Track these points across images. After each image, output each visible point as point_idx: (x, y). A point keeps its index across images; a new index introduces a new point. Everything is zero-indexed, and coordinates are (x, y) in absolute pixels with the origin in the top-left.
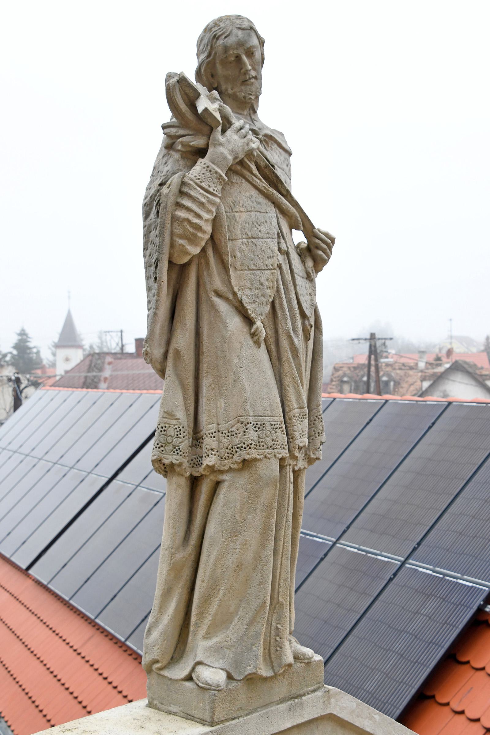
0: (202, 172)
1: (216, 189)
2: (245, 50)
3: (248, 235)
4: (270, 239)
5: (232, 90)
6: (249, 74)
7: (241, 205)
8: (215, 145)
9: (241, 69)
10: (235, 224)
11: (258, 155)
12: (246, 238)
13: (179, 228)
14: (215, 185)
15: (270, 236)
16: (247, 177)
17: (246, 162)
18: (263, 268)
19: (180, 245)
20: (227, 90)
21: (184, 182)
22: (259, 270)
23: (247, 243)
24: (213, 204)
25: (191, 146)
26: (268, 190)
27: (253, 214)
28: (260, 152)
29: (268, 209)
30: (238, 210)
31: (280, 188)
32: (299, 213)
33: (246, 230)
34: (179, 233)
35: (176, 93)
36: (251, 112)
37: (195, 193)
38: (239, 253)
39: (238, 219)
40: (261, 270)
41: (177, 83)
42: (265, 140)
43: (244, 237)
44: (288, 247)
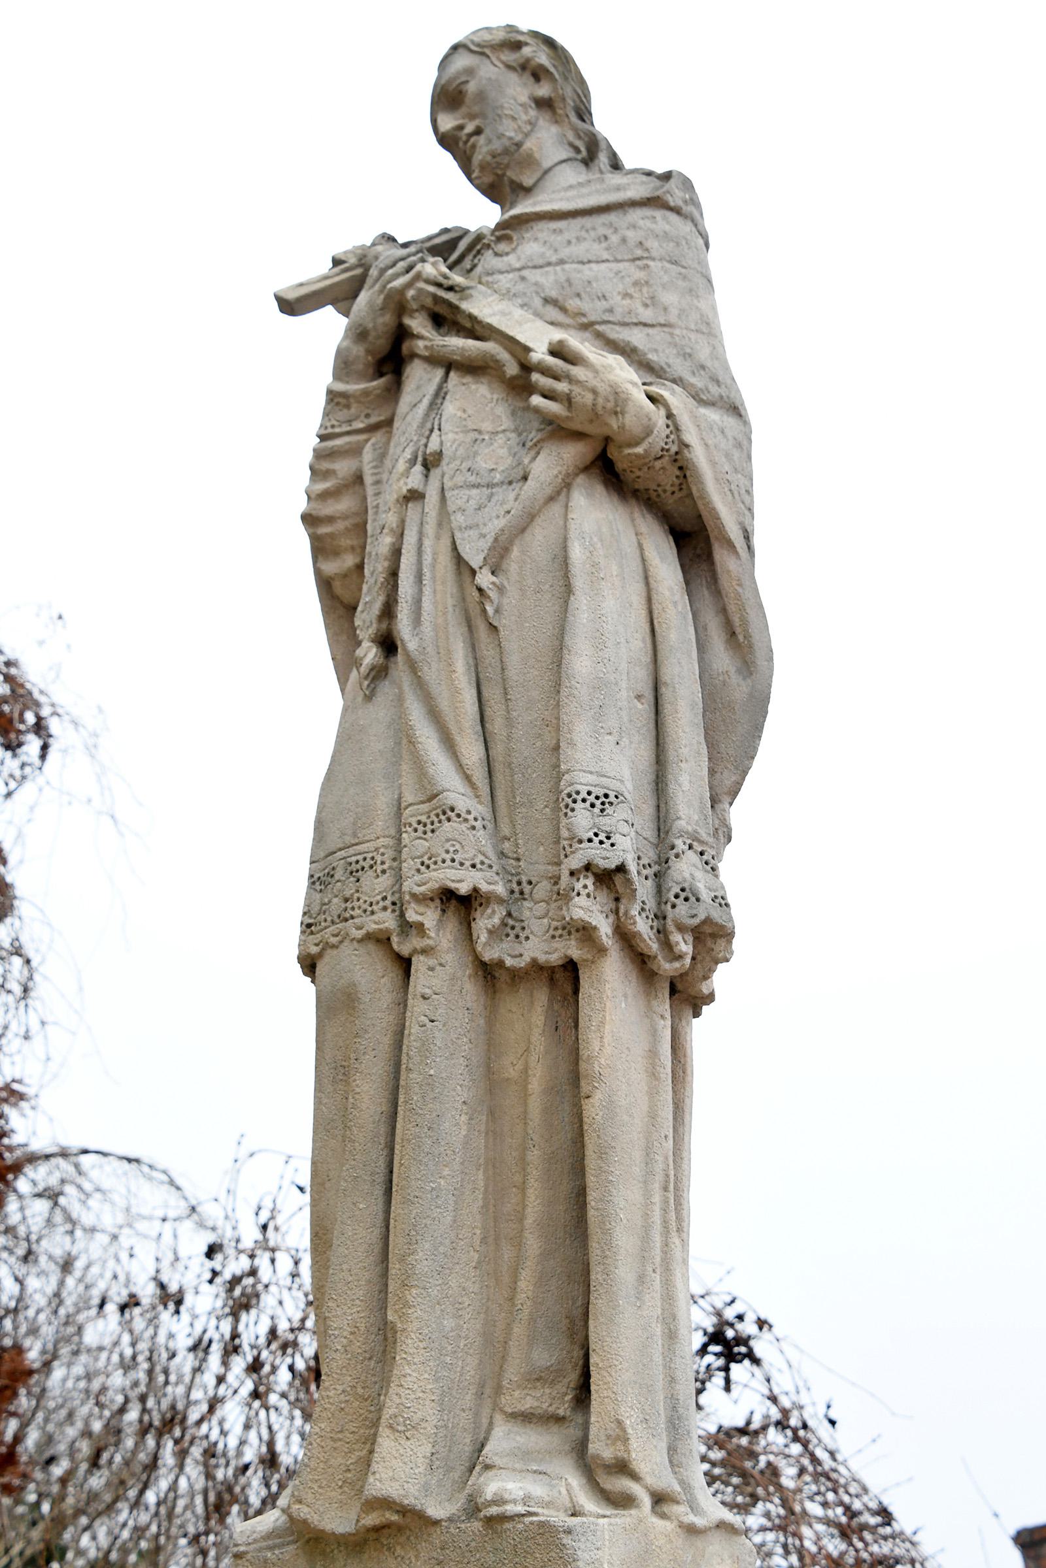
14: (330, 416)
32: (501, 344)
44: (442, 443)
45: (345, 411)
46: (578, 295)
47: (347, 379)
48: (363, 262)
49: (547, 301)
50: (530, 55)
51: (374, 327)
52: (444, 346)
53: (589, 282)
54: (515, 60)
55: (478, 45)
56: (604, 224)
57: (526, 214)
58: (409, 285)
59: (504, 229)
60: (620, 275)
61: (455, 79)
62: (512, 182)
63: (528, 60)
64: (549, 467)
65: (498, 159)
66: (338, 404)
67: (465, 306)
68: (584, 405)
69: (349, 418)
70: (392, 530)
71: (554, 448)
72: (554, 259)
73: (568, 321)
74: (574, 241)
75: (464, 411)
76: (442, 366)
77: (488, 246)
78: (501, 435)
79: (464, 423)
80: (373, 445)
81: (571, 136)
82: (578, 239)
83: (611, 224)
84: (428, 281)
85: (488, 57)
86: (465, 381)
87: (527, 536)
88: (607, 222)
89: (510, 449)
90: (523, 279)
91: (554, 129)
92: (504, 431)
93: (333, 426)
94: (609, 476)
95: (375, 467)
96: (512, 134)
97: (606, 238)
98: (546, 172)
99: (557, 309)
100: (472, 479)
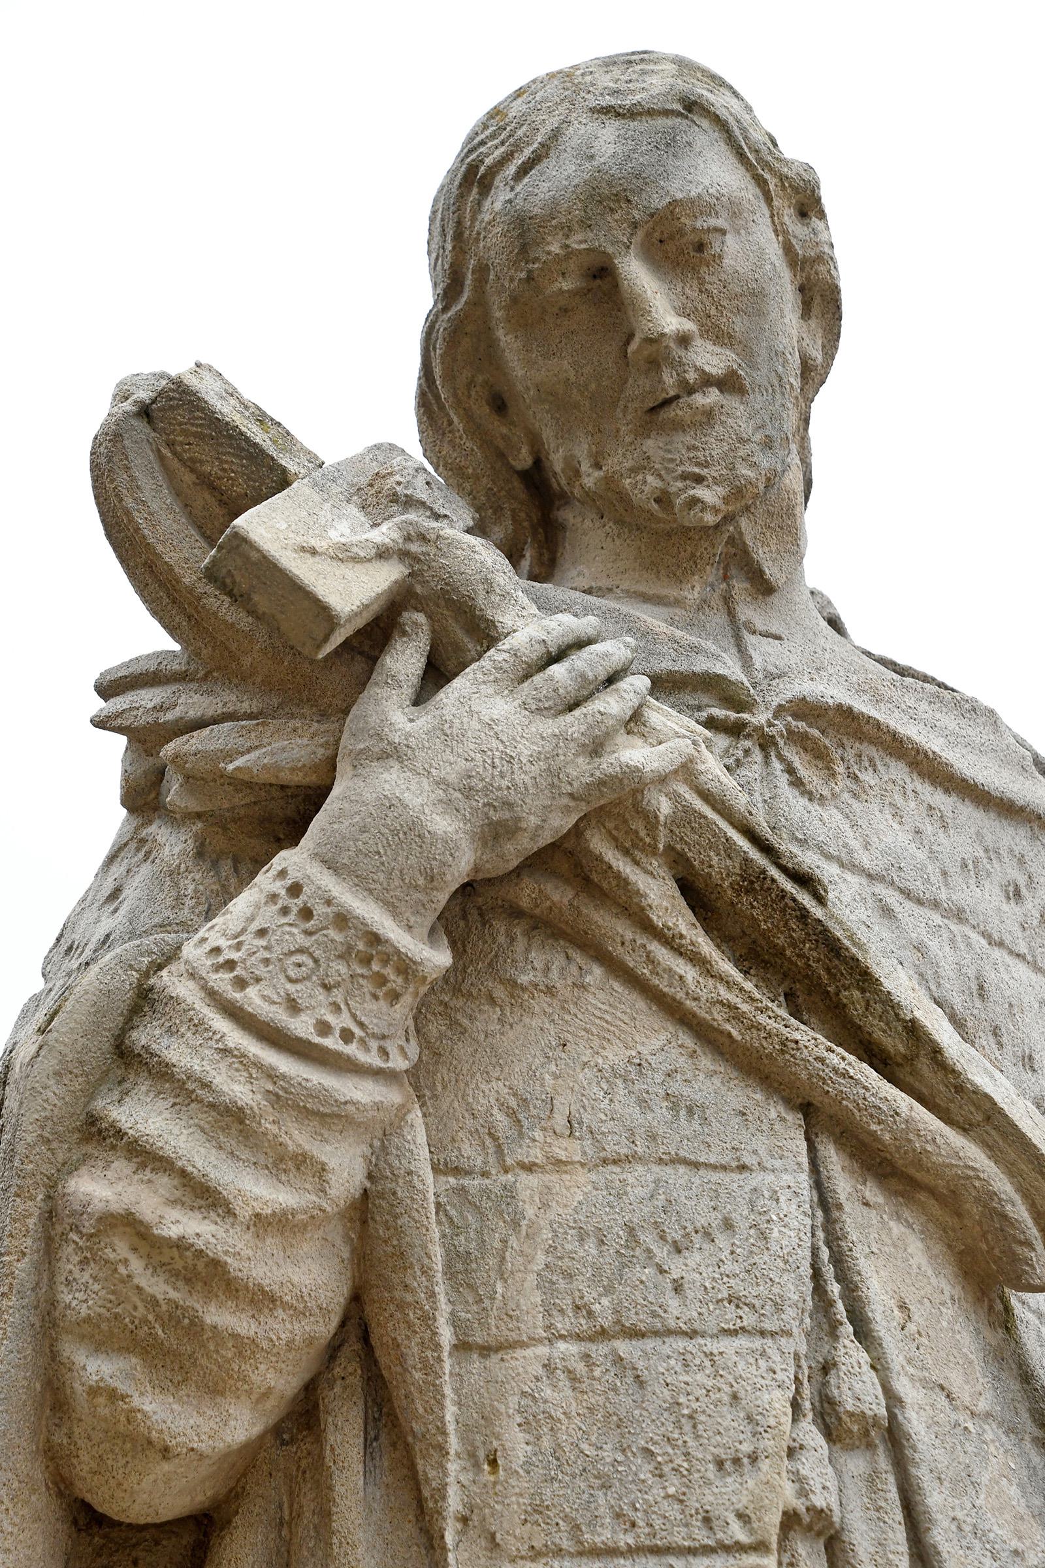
0: (255, 926)
1: (338, 1022)
2: (635, 225)
3: (590, 1314)
4: (742, 1342)
5: (598, 466)
7: (560, 1121)
8: (360, 758)
9: (630, 337)
10: (513, 1242)
11: (685, 816)
12: (579, 1338)
13: (86, 1276)
14: (338, 996)
15: (749, 1320)
16: (618, 951)
17: (599, 858)
18: (679, 1538)
19: (94, 1391)
20: (577, 473)
21: (151, 989)
22: (656, 1551)
23: (580, 1368)
24: (323, 1116)
25: (240, 783)
26: (759, 1027)
27: (639, 1179)
28: (706, 796)
29: (755, 1146)
30: (536, 1155)
31: (856, 1011)
32: (1011, 1171)
33: (581, 1283)
34: (84, 1311)
35: (133, 478)
36: (740, 586)
37: (195, 1049)
38: (521, 1436)
39: (530, 1212)
40: (667, 1550)
41: (140, 425)
42: (793, 737)
43: (562, 1325)
44: (893, 1399)
45: (383, 1004)
46: (996, 1032)
47: (412, 919)
48: (414, 548)
52: (845, 1075)
57: (878, 724)
58: (662, 780)
61: (710, 210)
90: (887, 912)
92: (988, 1415)
97: (1017, 894)
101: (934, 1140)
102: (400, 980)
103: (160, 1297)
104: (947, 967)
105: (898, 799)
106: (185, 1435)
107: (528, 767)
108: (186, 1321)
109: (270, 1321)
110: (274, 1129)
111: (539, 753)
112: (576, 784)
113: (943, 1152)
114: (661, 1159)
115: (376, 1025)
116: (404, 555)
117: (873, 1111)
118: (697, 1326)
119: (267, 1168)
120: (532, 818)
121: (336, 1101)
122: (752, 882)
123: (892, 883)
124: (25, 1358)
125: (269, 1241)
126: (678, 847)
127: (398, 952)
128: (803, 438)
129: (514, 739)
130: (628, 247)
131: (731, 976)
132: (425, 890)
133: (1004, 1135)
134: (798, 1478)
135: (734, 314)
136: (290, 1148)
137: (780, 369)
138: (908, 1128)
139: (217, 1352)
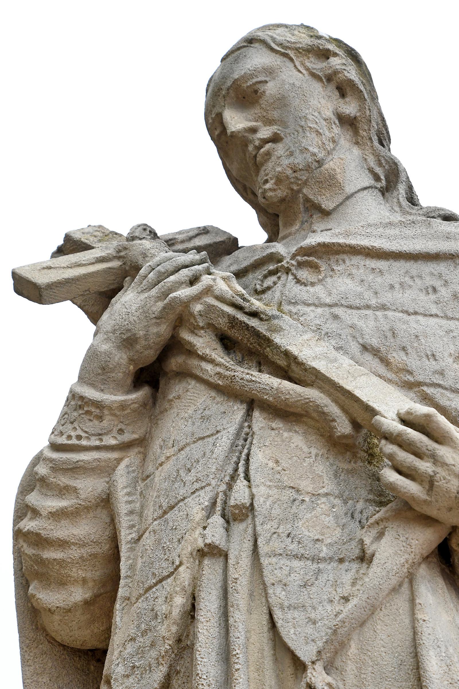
6: (252, 141)
14: (76, 425)
18: (165, 574)
24: (71, 469)
30: (163, 459)
31: (270, 355)
32: (329, 395)
44: (252, 497)
45: (96, 422)
46: (404, 349)
47: (102, 387)
48: (122, 254)
49: (365, 348)
50: (338, 67)
51: (146, 337)
53: (417, 336)
54: (321, 70)
55: (280, 45)
56: (432, 274)
57: (339, 245)
58: (197, 298)
59: (309, 256)
60: (451, 334)
61: (252, 76)
62: (307, 200)
63: (336, 73)
64: (396, 553)
65: (298, 175)
66: (88, 413)
67: (277, 339)
68: (448, 491)
69: (100, 432)
70: (183, 589)
71: (401, 531)
72: (373, 302)
73: (390, 375)
74: (397, 286)
75: (277, 462)
76: (242, 402)
77: (288, 271)
78: (324, 500)
79: (278, 476)
80: (127, 466)
81: (372, 162)
82: (401, 284)
83: (440, 276)
84: (221, 299)
85: (291, 60)
86: (274, 425)
87: (367, 629)
88: (436, 273)
89: (336, 517)
90: (336, 317)
91: (356, 151)
92: (327, 495)
93: (79, 437)
94: (444, 566)
95: (129, 494)
96: (316, 150)
97: (435, 290)
98: (348, 198)
99: (377, 360)
100: (293, 547)
101: (289, 393)
102: (98, 411)
103: (31, 554)
104: (367, 330)
105: (354, 271)
106: (53, 602)
107: (135, 313)
108: (39, 560)
109: (70, 551)
110: (55, 480)
111: (139, 306)
112: (156, 313)
113: (294, 396)
114: (194, 441)
115: (93, 430)
116: (119, 258)
117: (263, 391)
118: (185, 495)
119: (58, 496)
120: (141, 332)
121: (73, 462)
122: (232, 323)
123: (342, 305)
124: (20, 595)
125: (62, 522)
126: (210, 322)
127: (90, 400)
128: (372, 147)
129: (131, 306)
130: (224, 106)
131: (221, 362)
132: (103, 374)
133: (323, 381)
134: (204, 536)
135: (273, 111)
136: (61, 485)
137: (303, 123)
138: (278, 392)
139: (54, 568)
